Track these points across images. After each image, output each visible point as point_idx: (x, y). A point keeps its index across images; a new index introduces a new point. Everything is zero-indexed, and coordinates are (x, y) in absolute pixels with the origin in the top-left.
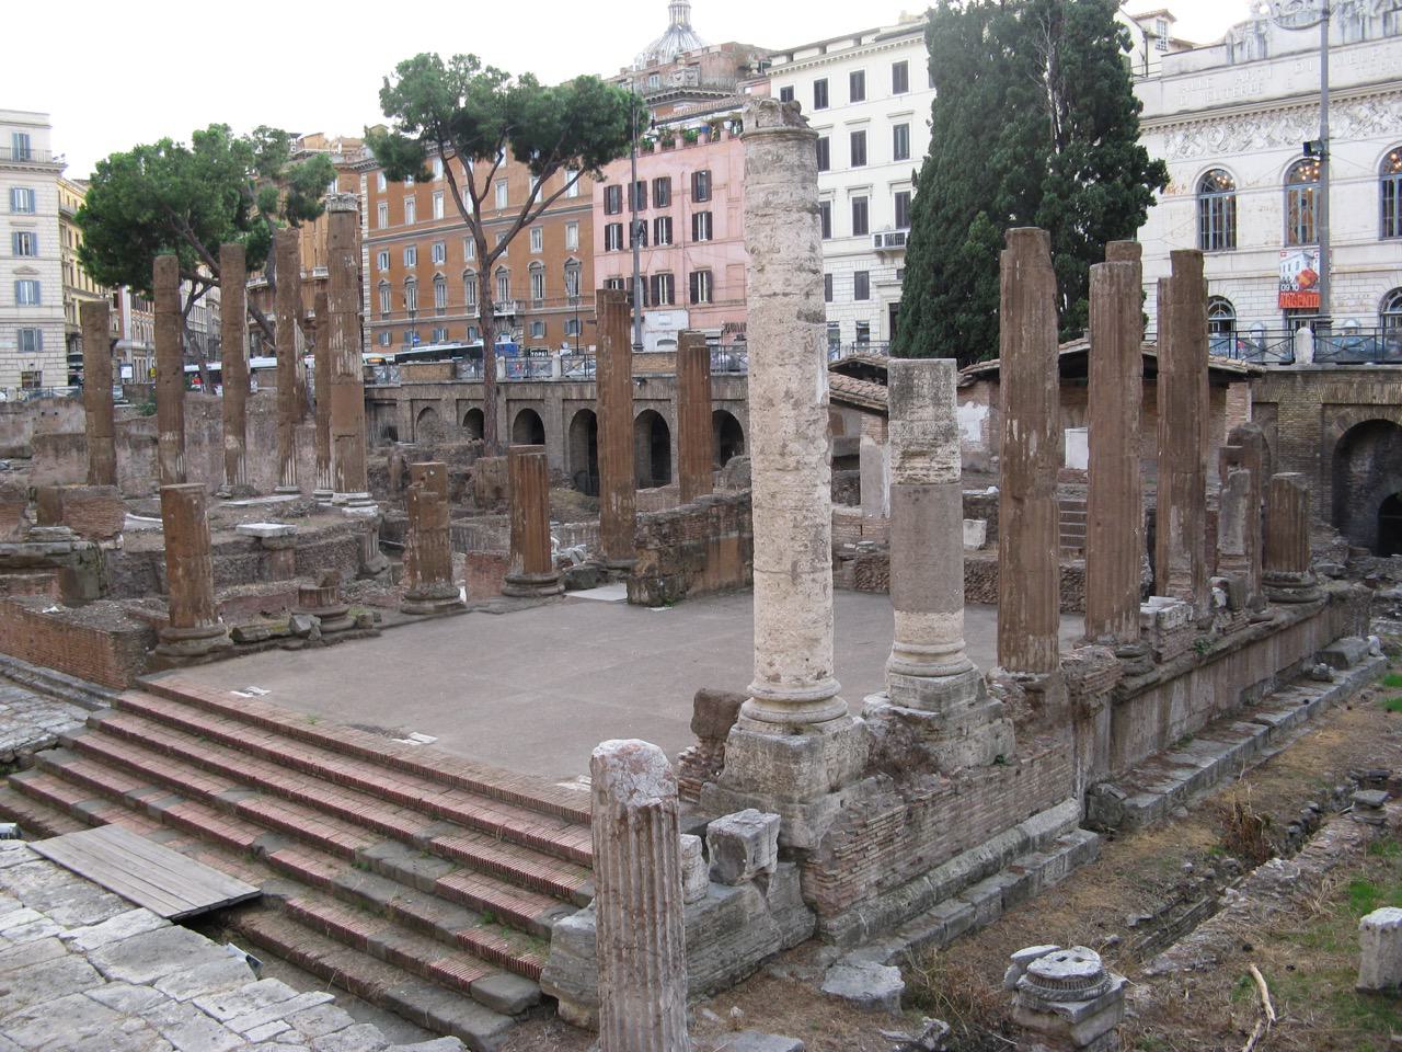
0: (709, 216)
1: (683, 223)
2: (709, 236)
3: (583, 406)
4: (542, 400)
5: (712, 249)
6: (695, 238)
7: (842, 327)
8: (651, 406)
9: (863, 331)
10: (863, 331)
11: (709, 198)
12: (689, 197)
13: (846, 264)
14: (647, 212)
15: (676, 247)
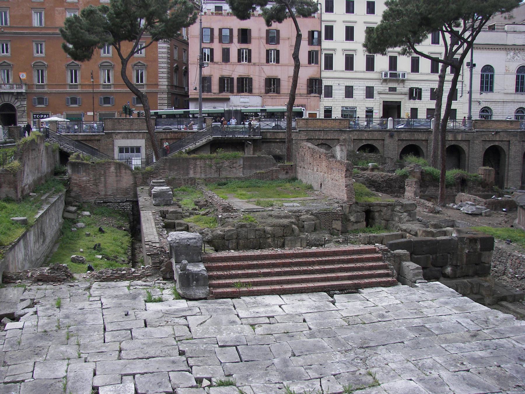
0: (278, 52)
1: (260, 53)
2: (278, 61)
3: (453, 143)
4: (426, 141)
5: (279, 68)
6: (268, 61)
7: (358, 110)
8: (497, 143)
9: (369, 112)
10: (369, 112)
11: (278, 43)
12: (264, 41)
13: (363, 83)
14: (233, 45)
15: (254, 64)
